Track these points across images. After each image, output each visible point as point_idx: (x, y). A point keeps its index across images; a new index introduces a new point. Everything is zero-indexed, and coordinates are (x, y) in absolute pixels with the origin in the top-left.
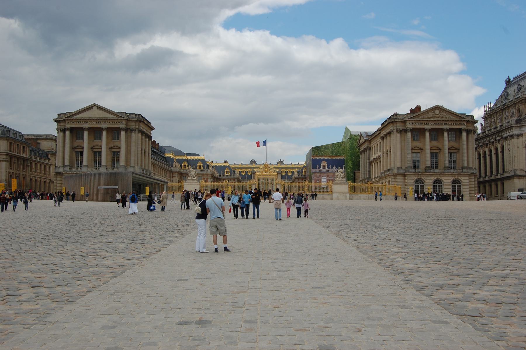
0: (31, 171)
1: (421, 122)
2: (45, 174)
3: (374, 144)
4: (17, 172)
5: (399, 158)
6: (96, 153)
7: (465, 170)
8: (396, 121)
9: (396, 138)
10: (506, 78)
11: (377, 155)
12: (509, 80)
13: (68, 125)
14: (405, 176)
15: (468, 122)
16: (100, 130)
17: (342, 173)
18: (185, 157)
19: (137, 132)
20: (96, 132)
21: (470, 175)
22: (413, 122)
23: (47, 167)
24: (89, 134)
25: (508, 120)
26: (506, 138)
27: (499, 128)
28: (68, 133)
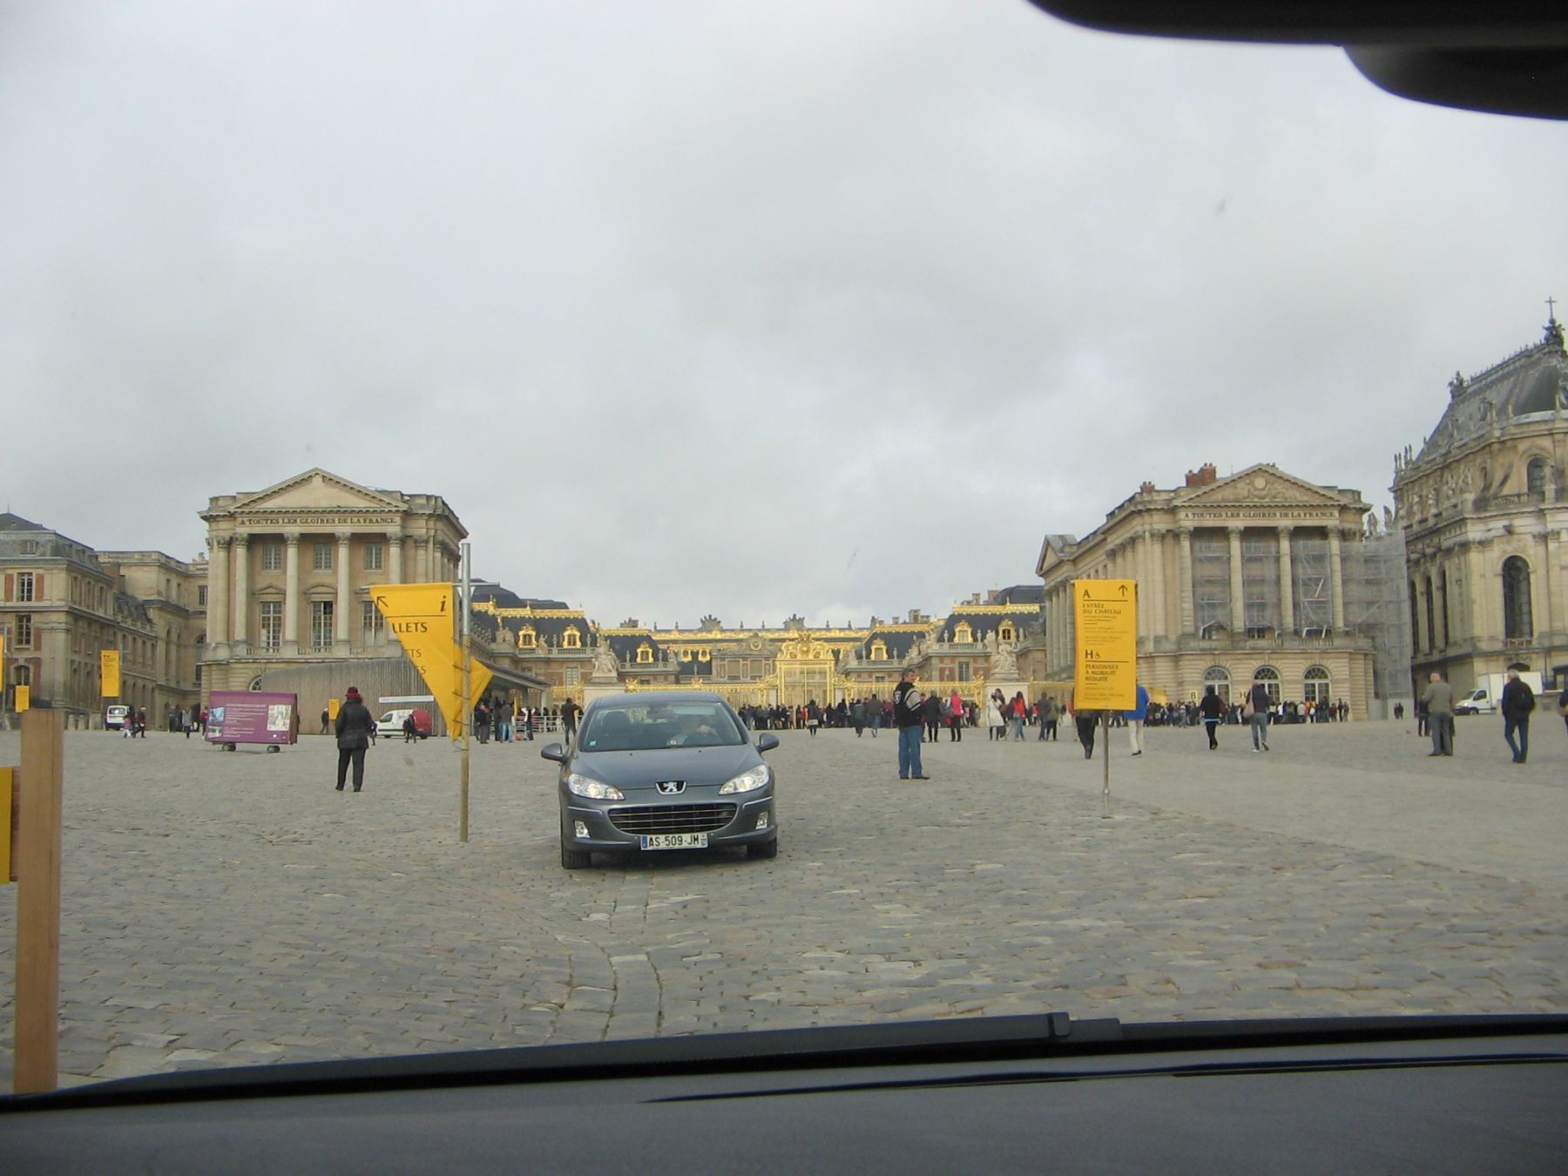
2: (144, 664)
8: (1149, 510)
9: (1150, 555)
10: (1451, 377)
12: (1461, 382)
13: (244, 531)
15: (1343, 509)
16: (331, 539)
17: (1010, 653)
18: (526, 612)
19: (431, 545)
20: (318, 544)
23: (149, 644)
24: (300, 554)
25: (1453, 501)
26: (1449, 551)
27: (1431, 522)
28: (241, 552)
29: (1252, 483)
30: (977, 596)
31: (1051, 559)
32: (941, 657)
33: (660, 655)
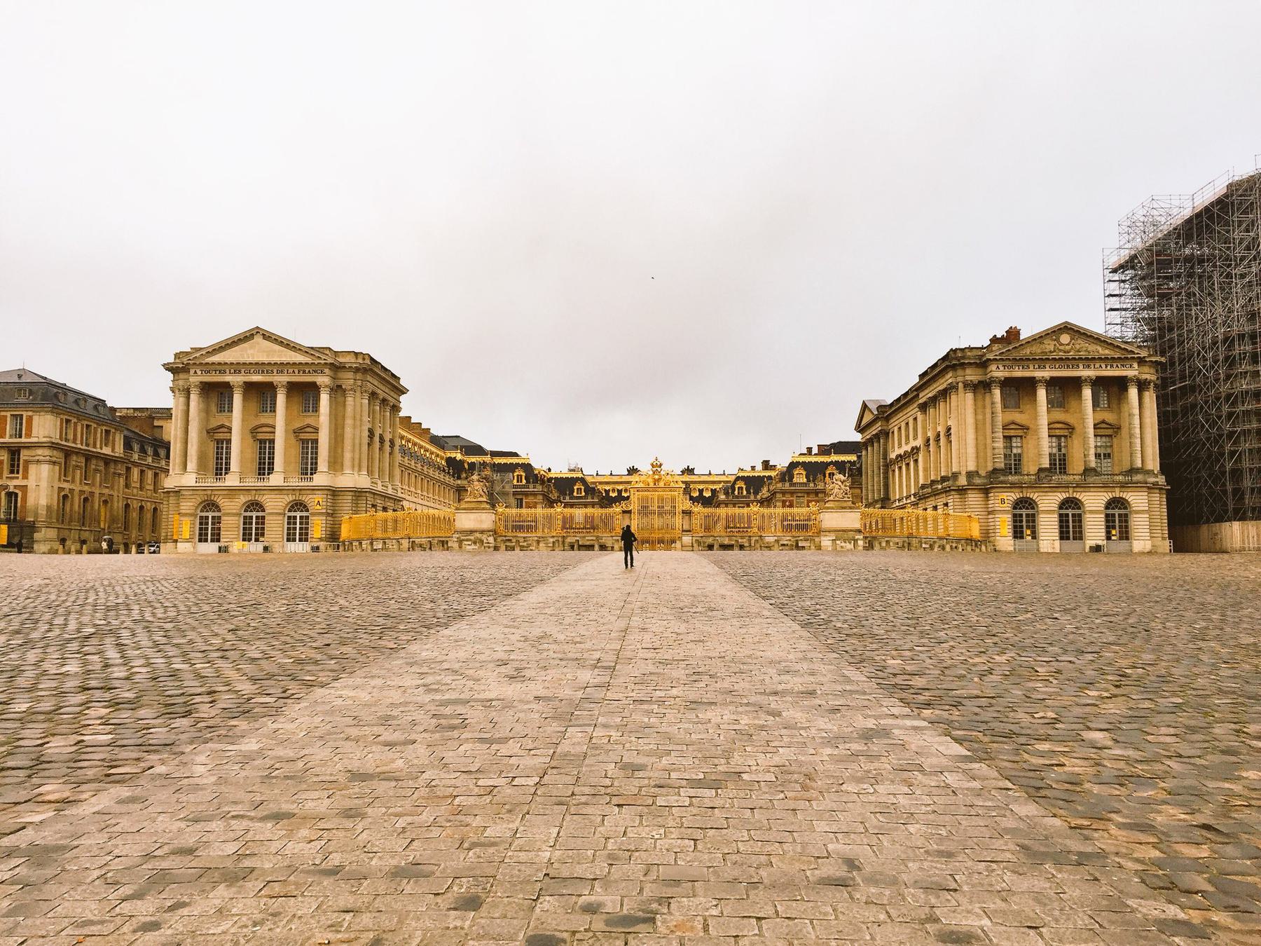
0: (127, 486)
1: (1026, 363)
3: (896, 423)
4: (86, 488)
5: (971, 450)
6: (262, 442)
7: (1138, 477)
9: (964, 402)
11: (908, 448)
14: (986, 491)
18: (488, 459)
19: (358, 394)
20: (261, 393)
21: (1151, 488)
22: (1007, 363)
28: (194, 397)
29: (1057, 340)
30: (810, 450)
31: (868, 418)
32: (784, 493)
33: (590, 490)
